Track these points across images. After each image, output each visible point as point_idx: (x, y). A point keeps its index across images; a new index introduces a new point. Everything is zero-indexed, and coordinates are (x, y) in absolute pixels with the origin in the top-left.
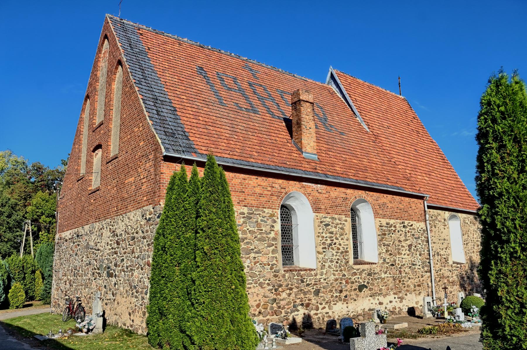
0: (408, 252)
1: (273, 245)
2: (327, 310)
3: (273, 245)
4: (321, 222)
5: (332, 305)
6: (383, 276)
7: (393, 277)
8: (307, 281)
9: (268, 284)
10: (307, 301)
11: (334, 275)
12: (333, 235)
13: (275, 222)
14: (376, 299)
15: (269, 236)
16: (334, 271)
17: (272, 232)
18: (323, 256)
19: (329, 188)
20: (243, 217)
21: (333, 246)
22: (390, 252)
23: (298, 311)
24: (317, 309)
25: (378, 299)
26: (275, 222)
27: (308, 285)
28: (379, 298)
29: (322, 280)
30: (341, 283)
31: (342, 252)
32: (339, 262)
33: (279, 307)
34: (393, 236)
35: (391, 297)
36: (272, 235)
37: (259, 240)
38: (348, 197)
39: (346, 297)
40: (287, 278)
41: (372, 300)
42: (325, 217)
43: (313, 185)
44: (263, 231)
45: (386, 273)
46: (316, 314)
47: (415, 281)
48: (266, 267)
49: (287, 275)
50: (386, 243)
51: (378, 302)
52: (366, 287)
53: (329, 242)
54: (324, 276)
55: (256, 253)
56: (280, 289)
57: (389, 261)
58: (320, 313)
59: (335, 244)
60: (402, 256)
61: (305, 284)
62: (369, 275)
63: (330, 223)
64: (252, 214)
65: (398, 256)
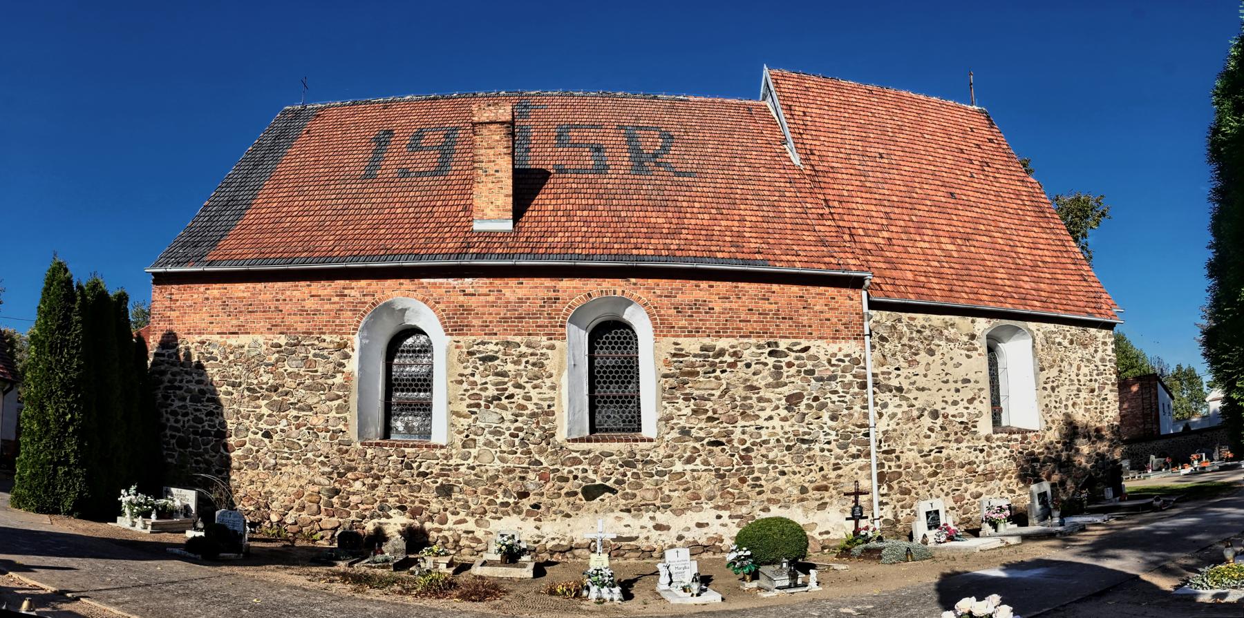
0: (784, 413)
1: (339, 397)
2: (471, 525)
4: (471, 354)
6: (678, 467)
7: (717, 470)
8: (420, 466)
9: (323, 463)
10: (417, 504)
11: (502, 460)
12: (506, 379)
13: (347, 356)
15: (330, 382)
17: (339, 375)
18: (470, 421)
19: (498, 282)
21: (504, 401)
23: (389, 517)
24: (444, 521)
26: (347, 356)
28: (658, 515)
29: (463, 469)
30: (523, 478)
31: (533, 415)
33: (345, 505)
34: (722, 376)
35: (708, 515)
36: (339, 379)
37: (309, 388)
38: (560, 295)
39: (536, 506)
40: (368, 456)
42: (483, 343)
43: (450, 280)
45: (690, 460)
46: (440, 531)
47: (808, 478)
48: (322, 434)
49: (369, 451)
50: (696, 393)
51: (651, 524)
52: (613, 491)
53: (492, 391)
54: (470, 461)
55: (300, 409)
56: (349, 475)
57: (702, 434)
58: (449, 530)
59: (511, 396)
60: (761, 422)
61: (415, 472)
63: (500, 355)
64: (295, 345)
65: (741, 423)
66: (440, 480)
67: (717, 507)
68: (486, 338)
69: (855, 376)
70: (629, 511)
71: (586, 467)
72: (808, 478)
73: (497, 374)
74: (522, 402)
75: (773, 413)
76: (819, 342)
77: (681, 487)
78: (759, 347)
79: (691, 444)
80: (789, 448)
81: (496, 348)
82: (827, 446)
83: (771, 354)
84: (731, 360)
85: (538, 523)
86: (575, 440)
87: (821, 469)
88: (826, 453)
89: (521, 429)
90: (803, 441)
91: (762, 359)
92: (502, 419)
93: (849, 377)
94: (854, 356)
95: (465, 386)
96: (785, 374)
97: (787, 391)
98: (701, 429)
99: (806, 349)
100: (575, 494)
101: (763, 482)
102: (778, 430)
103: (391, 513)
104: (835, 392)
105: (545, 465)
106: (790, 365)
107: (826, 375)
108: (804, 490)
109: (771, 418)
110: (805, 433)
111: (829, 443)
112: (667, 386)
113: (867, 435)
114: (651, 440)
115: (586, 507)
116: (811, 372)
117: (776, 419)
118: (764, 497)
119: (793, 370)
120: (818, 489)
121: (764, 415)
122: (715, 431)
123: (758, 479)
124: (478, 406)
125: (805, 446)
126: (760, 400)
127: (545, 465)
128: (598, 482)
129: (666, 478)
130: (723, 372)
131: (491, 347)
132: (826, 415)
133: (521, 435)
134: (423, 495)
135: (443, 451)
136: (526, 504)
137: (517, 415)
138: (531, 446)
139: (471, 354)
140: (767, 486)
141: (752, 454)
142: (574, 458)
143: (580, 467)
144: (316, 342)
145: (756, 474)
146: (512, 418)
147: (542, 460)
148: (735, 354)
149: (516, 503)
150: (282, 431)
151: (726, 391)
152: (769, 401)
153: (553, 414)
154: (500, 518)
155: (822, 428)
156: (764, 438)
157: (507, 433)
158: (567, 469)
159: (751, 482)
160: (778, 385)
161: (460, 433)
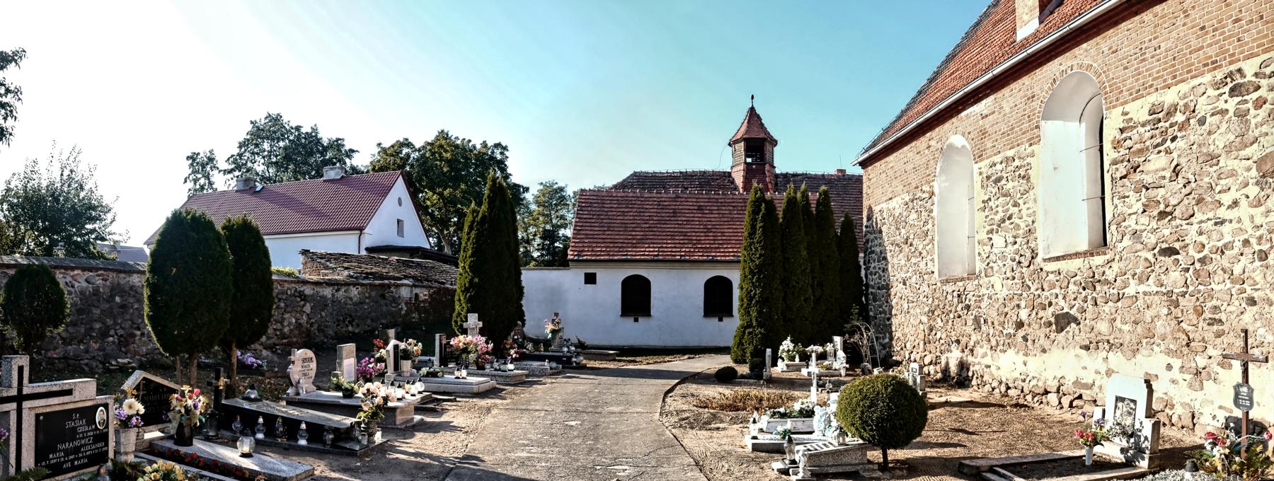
0: (1253, 191)
60: (1222, 213)
67: (1169, 352)
78: (1217, 85)
83: (1234, 91)
85: (1025, 358)
86: (1050, 260)
96: (1253, 122)
102: (1247, 224)
117: (1244, 202)
121: (1227, 199)
141: (1210, 268)
152: (1233, 174)
159: (1207, 315)
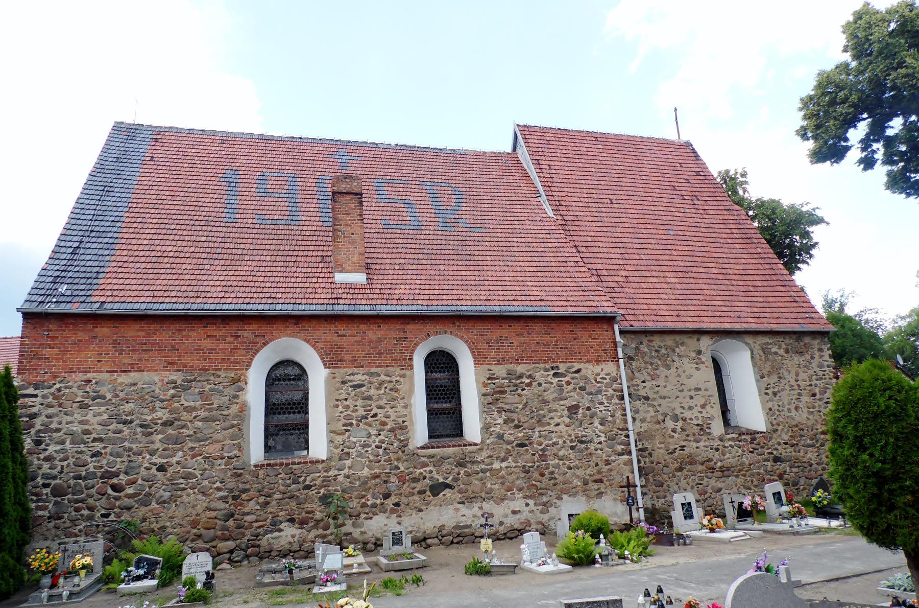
0: (567, 420)
1: (233, 426)
3: (233, 426)
5: (361, 519)
6: (496, 465)
7: (524, 467)
8: (305, 480)
9: (218, 489)
10: (304, 515)
11: (370, 468)
14: (476, 509)
16: (370, 461)
20: (173, 388)
22: (516, 422)
25: (481, 508)
27: (308, 487)
28: (485, 505)
29: (341, 478)
30: (386, 482)
31: (392, 430)
32: (383, 445)
35: (518, 504)
37: (205, 420)
39: (397, 505)
41: (463, 509)
42: (352, 374)
44: (214, 406)
47: (588, 472)
50: (507, 407)
53: (361, 412)
54: (346, 471)
56: (244, 496)
57: (512, 438)
59: (375, 415)
60: (552, 428)
61: (301, 486)
62: (460, 465)
63: (366, 383)
66: (322, 491)
67: (526, 497)
68: (356, 370)
69: (615, 391)
70: (463, 503)
71: (431, 468)
72: (588, 472)
73: (364, 399)
74: (384, 419)
75: (559, 421)
76: (587, 365)
77: (500, 481)
79: (505, 446)
80: (572, 448)
81: (363, 378)
82: (600, 446)
83: (555, 375)
84: (528, 381)
87: (597, 465)
88: (599, 452)
89: (382, 442)
90: (582, 442)
91: (549, 380)
92: (369, 435)
93: (611, 392)
94: (613, 375)
95: (340, 409)
97: (568, 403)
98: (511, 434)
99: (578, 371)
100: (424, 492)
101: (557, 476)
102: (564, 433)
103: (281, 526)
104: (602, 403)
105: (402, 469)
106: (568, 383)
107: (594, 390)
108: (586, 483)
109: (558, 425)
110: (583, 436)
111: (600, 443)
112: (486, 402)
113: (627, 436)
114: (476, 445)
115: (433, 503)
116: (582, 389)
118: (558, 487)
119: (570, 387)
120: (595, 481)
122: (520, 435)
123: (552, 473)
124: (351, 424)
125: (583, 446)
126: (550, 411)
127: (402, 469)
128: (441, 480)
129: (488, 474)
130: (523, 390)
131: (360, 377)
132: (596, 423)
133: (383, 445)
134: (308, 506)
135: (324, 465)
136: (390, 502)
137: (380, 430)
138: (391, 455)
139: (344, 383)
140: (560, 479)
142: (423, 462)
143: (428, 469)
144: (212, 378)
145: (551, 469)
146: (375, 432)
147: (400, 465)
148: (530, 376)
149: (382, 504)
150: (178, 463)
151: (525, 405)
153: (407, 427)
154: (371, 518)
155: (594, 432)
156: (554, 440)
157: (373, 446)
158: (418, 471)
160: (561, 399)
161: (337, 448)
